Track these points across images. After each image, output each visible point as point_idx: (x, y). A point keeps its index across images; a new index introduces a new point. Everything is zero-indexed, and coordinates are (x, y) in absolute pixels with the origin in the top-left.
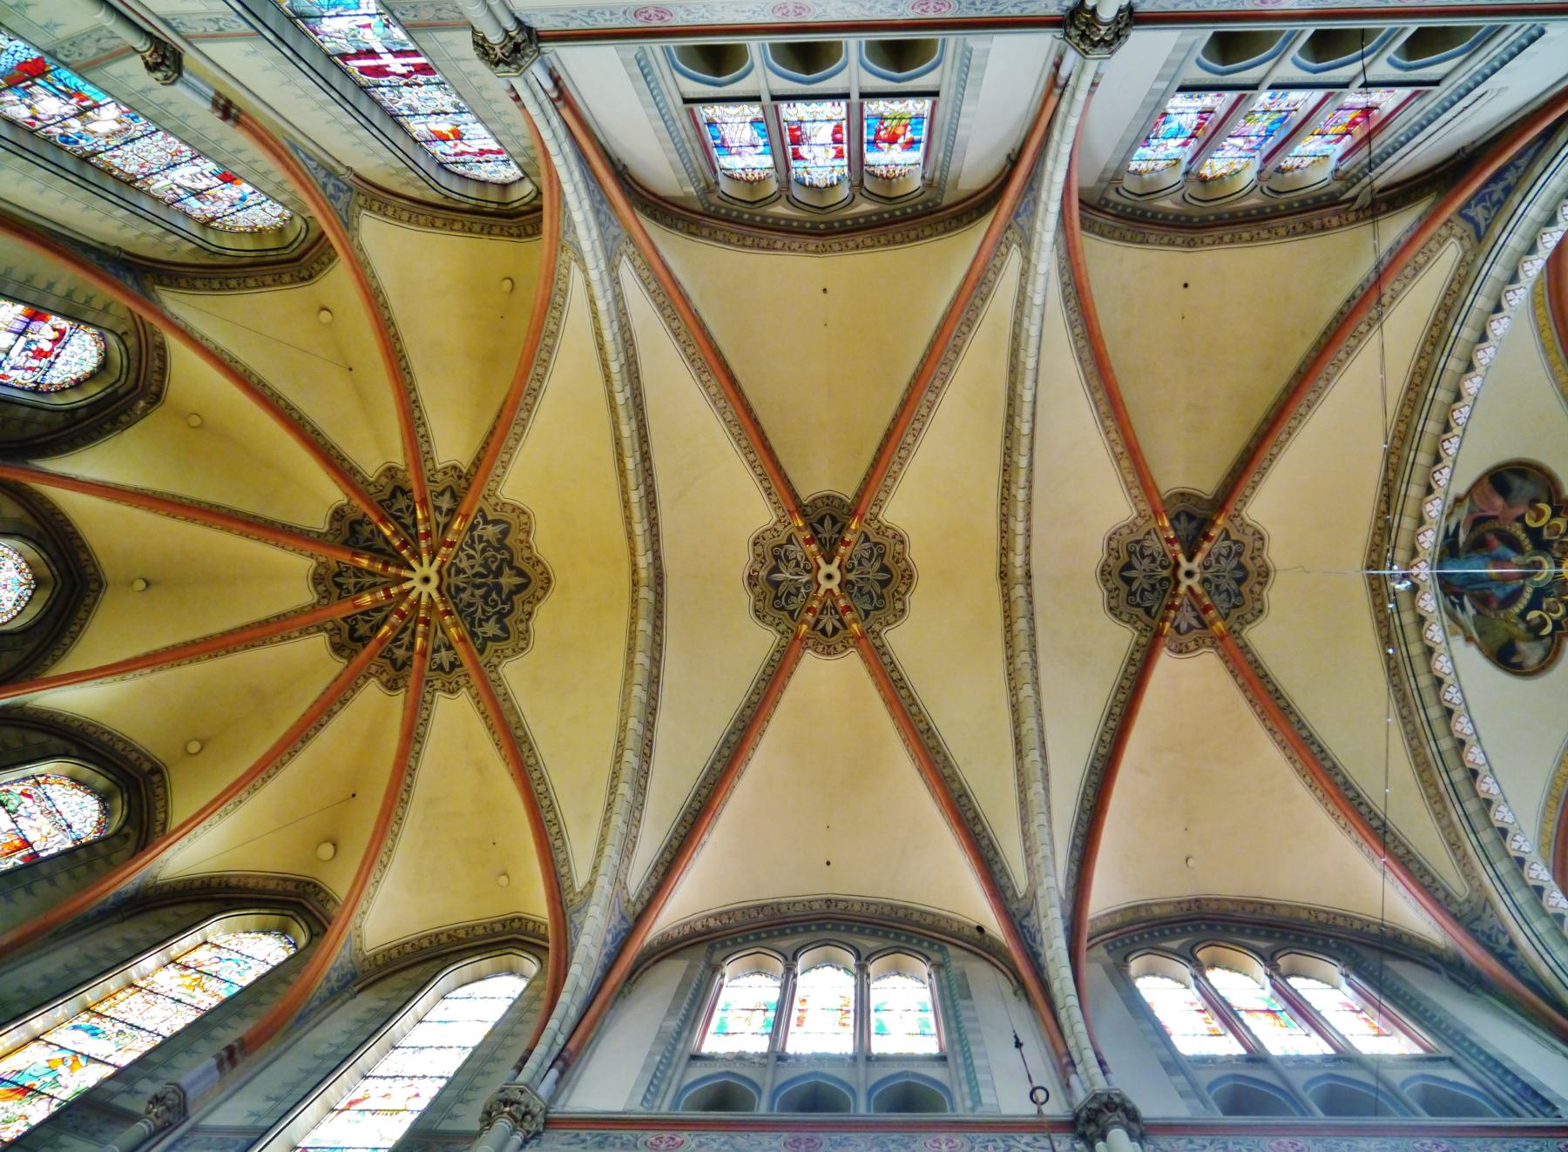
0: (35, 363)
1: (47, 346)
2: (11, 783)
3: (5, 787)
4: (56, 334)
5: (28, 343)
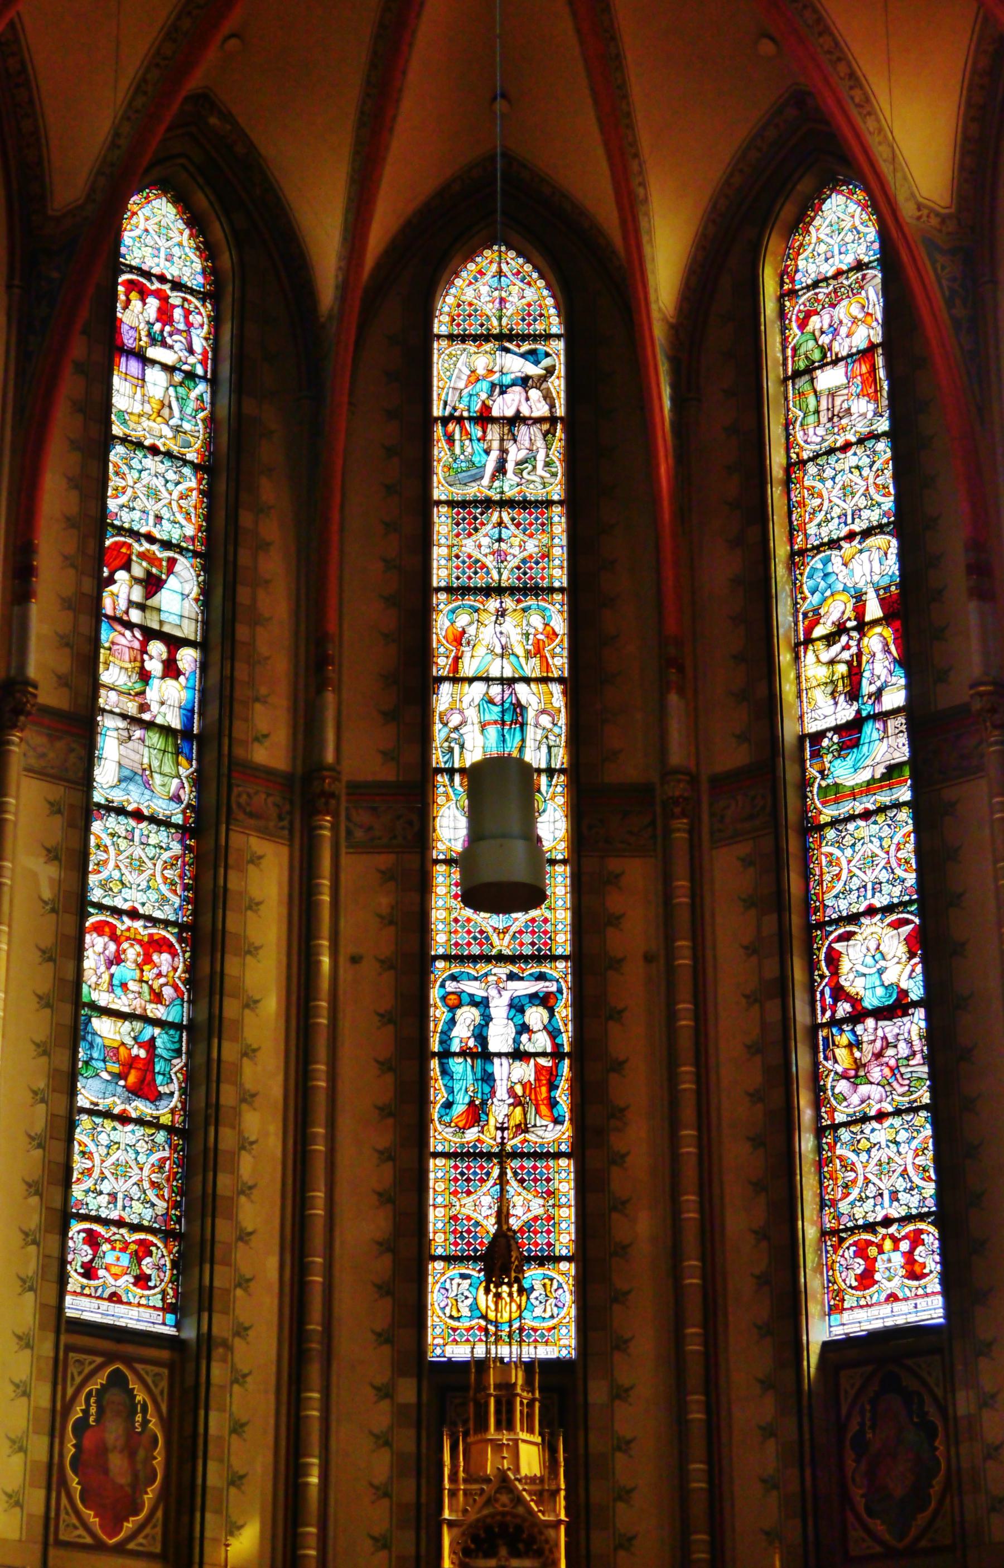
0: (178, 314)
1: (153, 303)
2: (784, 341)
3: (789, 352)
4: (134, 295)
5: (153, 341)
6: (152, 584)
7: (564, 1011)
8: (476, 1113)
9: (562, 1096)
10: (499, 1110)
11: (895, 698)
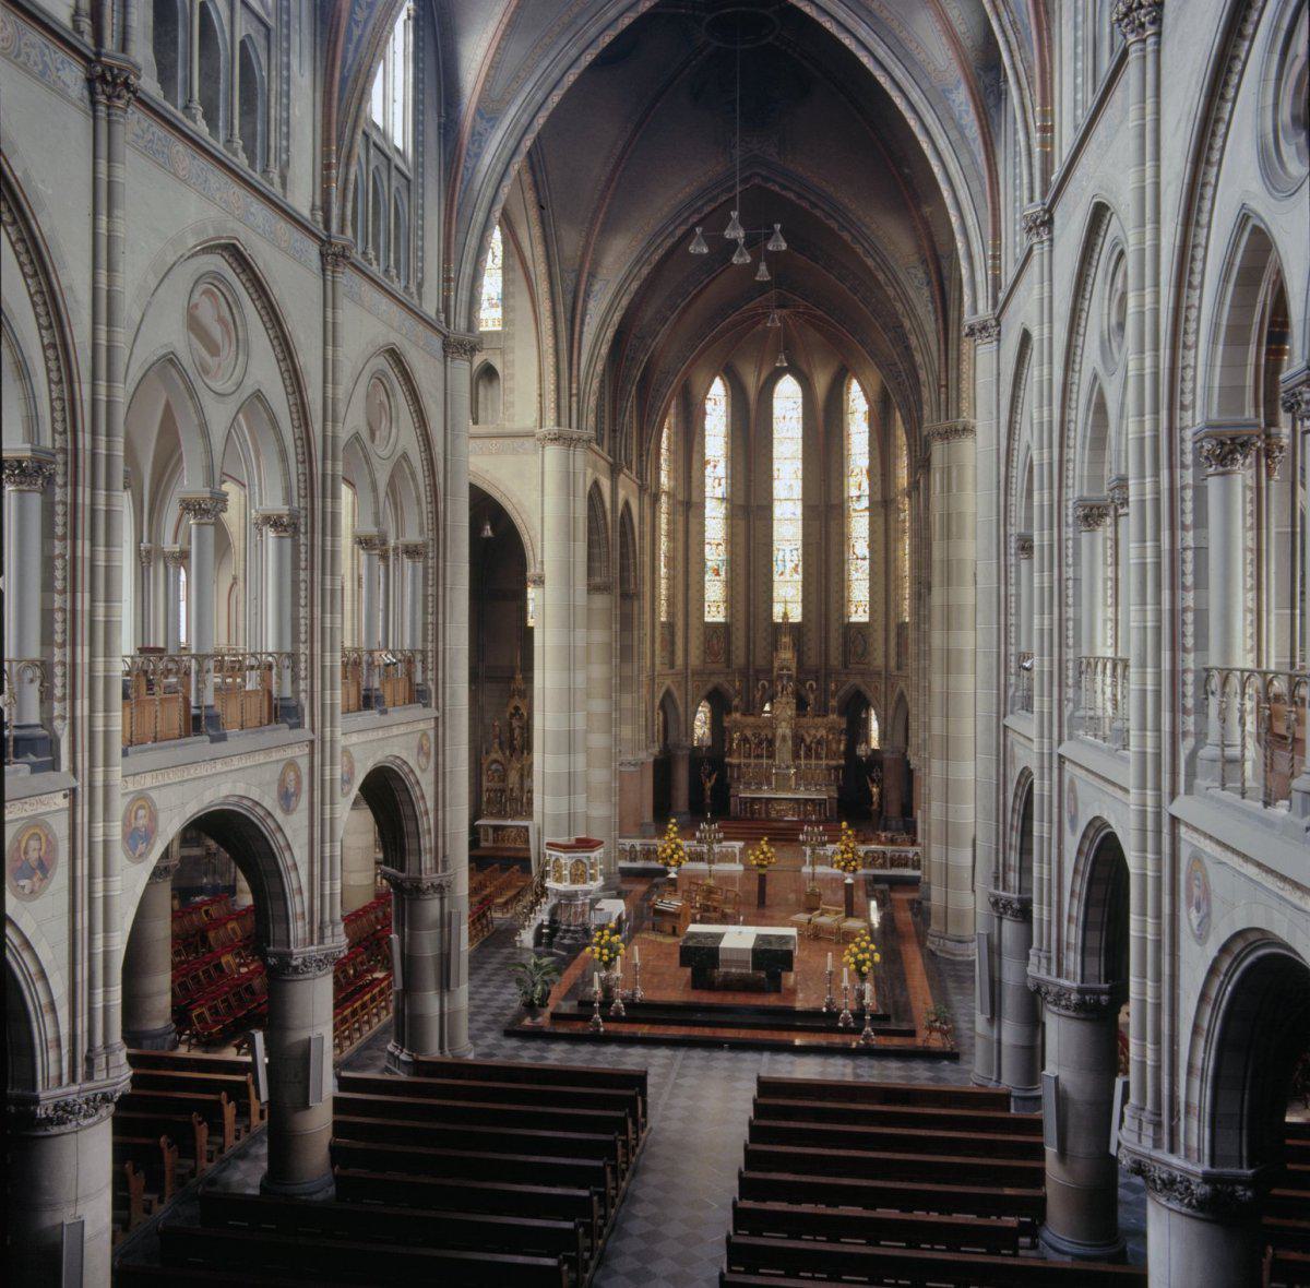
6: (715, 467)
7: (800, 551)
8: (782, 574)
9: (800, 569)
10: (787, 571)
11: (867, 492)
